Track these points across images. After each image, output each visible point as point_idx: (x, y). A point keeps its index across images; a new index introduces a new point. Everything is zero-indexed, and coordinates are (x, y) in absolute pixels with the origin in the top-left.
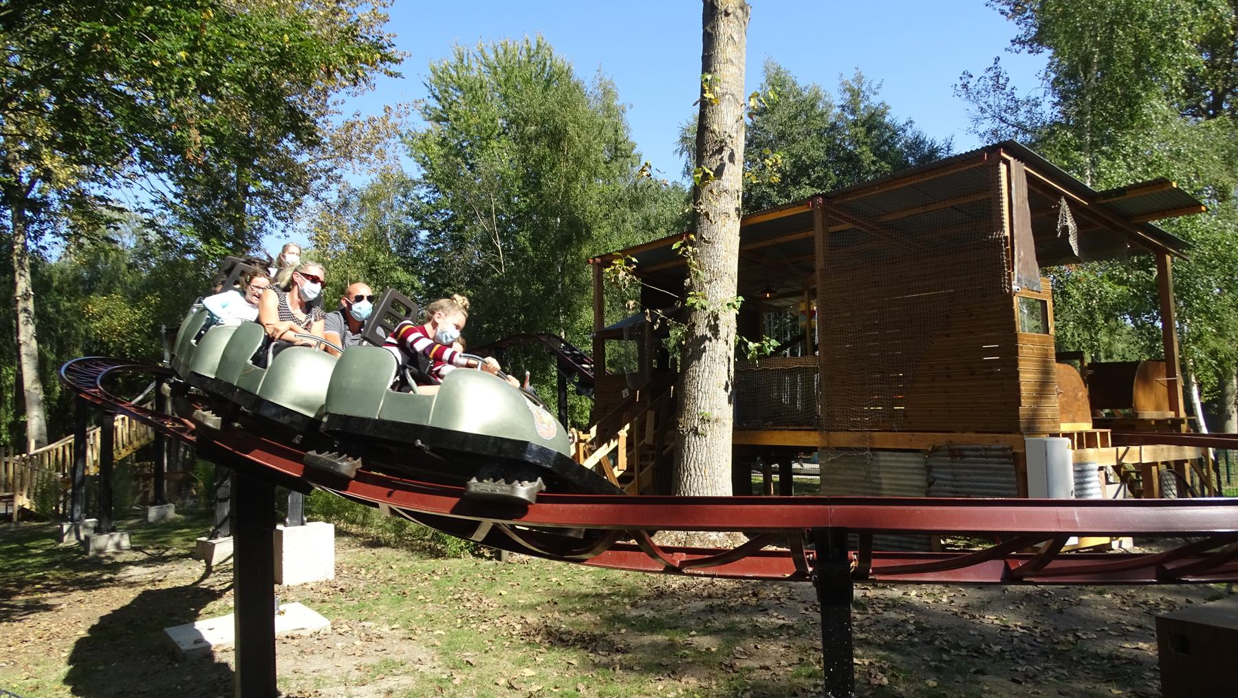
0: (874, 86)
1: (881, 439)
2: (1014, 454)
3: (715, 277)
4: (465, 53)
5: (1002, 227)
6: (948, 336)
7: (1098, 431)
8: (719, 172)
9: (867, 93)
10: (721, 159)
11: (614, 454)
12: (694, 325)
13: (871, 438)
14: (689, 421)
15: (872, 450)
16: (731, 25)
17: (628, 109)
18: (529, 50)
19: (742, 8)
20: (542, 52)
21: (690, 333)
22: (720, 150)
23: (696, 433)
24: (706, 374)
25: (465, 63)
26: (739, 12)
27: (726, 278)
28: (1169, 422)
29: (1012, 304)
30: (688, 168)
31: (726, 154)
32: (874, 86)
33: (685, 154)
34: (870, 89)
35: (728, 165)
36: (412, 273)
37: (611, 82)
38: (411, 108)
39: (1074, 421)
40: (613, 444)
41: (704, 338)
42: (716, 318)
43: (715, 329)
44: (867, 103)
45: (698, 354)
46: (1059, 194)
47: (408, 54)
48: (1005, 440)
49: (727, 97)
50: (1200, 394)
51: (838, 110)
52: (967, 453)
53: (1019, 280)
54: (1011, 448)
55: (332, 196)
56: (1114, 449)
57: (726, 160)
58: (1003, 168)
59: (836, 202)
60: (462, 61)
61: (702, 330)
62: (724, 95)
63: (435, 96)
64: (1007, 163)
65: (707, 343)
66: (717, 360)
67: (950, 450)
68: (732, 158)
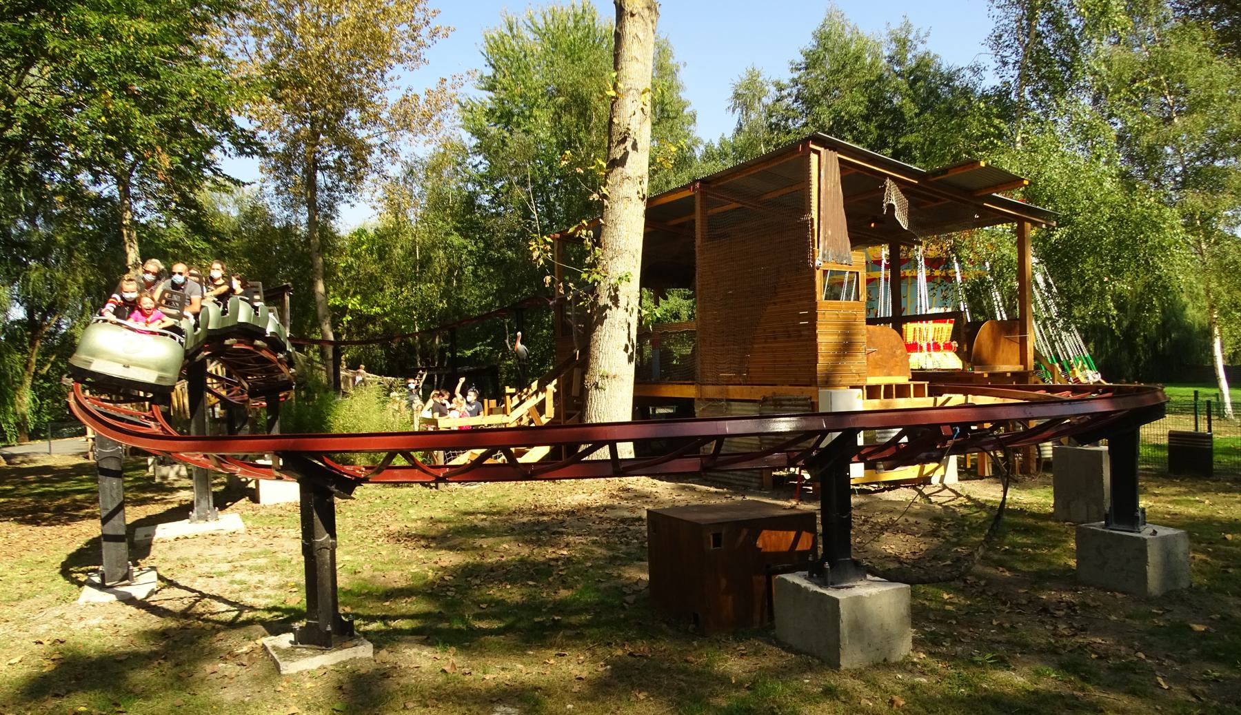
0: (922, 34)
1: (735, 391)
2: (813, 403)
3: (618, 253)
4: (515, 20)
5: (810, 210)
6: (775, 304)
7: (912, 384)
8: (622, 162)
9: (915, 42)
10: (625, 149)
11: (541, 408)
12: (598, 296)
13: (727, 391)
14: (593, 378)
15: (729, 400)
16: (637, 24)
17: (681, 67)
18: (576, 15)
19: (649, 8)
20: (588, 17)
21: (594, 304)
22: (624, 140)
23: (597, 388)
24: (607, 338)
25: (515, 31)
26: (646, 12)
27: (626, 255)
28: (1009, 375)
29: (814, 277)
30: (741, 125)
31: (629, 144)
32: (922, 34)
33: (738, 110)
34: (917, 37)
35: (632, 153)
36: (466, 237)
37: (666, 41)
38: (465, 78)
39: (889, 375)
40: (541, 396)
41: (606, 307)
42: (616, 290)
43: (615, 300)
44: (913, 52)
45: (601, 321)
46: (886, 176)
47: (452, 28)
48: (807, 392)
49: (631, 92)
50: (1222, 347)
51: (885, 61)
52: (784, 403)
53: (824, 256)
54: (810, 398)
55: (395, 170)
56: (932, 399)
57: (629, 149)
58: (814, 158)
59: (713, 186)
60: (511, 29)
61: (604, 300)
62: (629, 90)
63: (491, 64)
64: (818, 153)
65: (608, 311)
66: (617, 326)
67: (774, 400)
68: (635, 147)
